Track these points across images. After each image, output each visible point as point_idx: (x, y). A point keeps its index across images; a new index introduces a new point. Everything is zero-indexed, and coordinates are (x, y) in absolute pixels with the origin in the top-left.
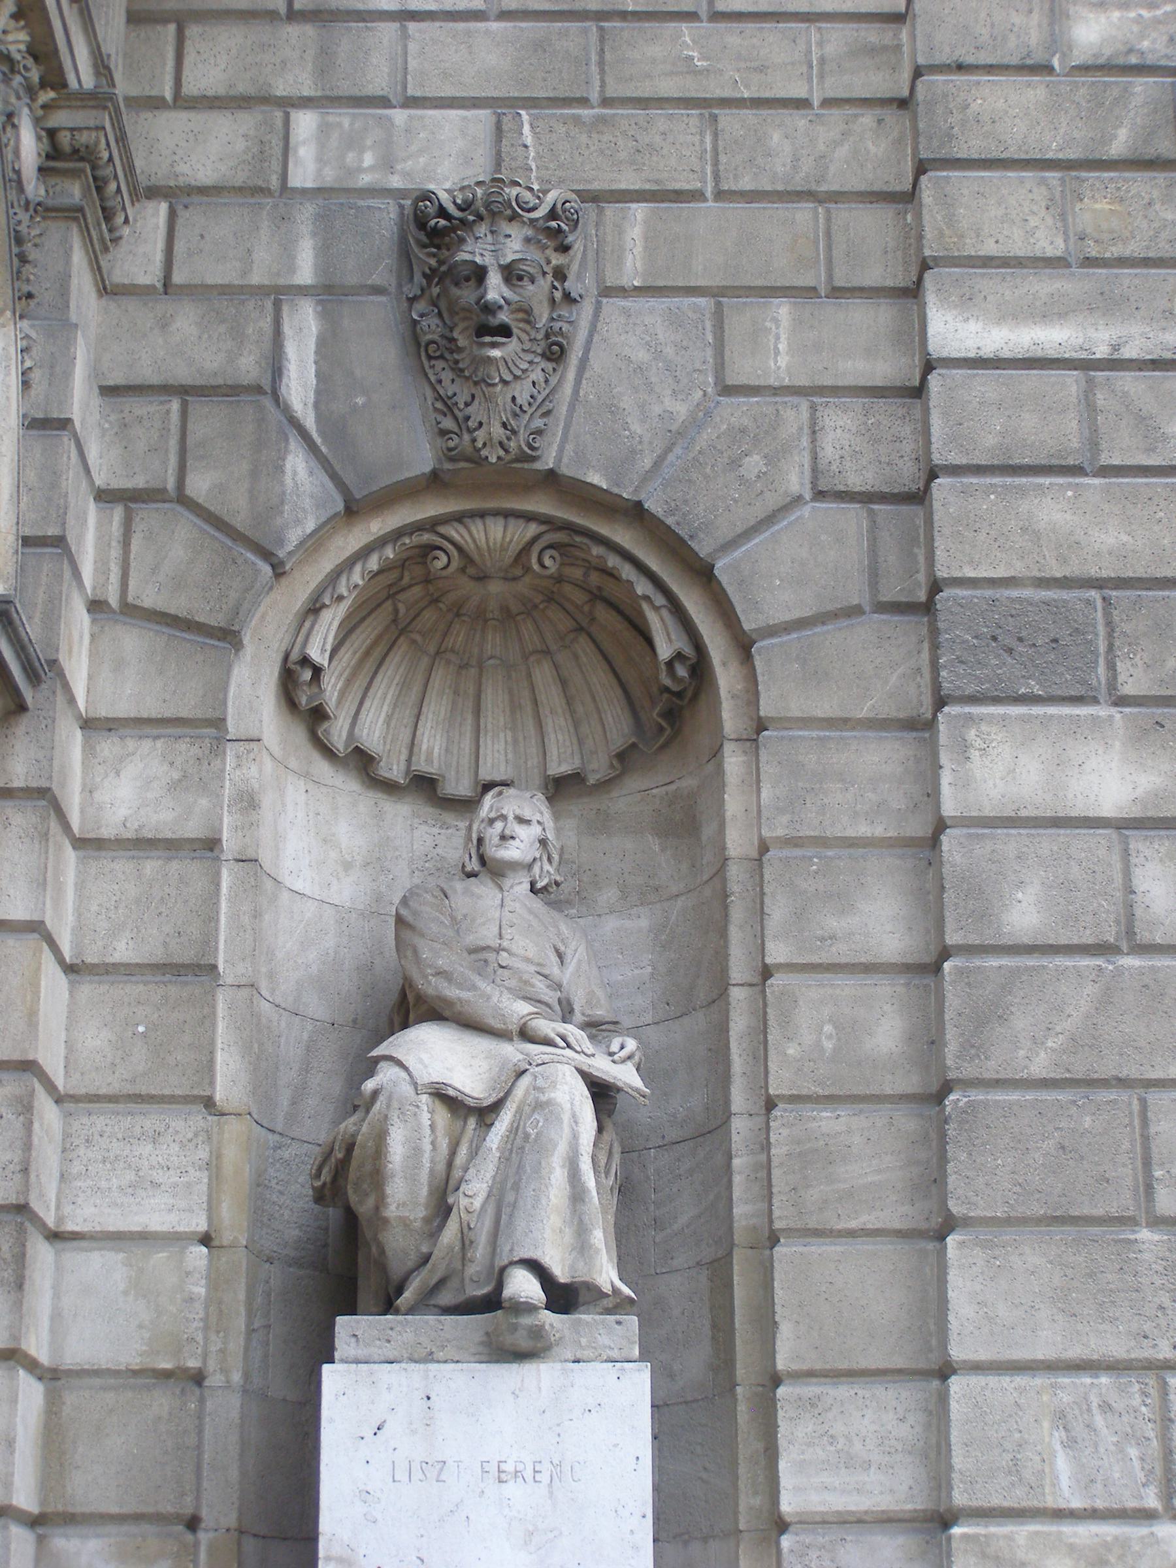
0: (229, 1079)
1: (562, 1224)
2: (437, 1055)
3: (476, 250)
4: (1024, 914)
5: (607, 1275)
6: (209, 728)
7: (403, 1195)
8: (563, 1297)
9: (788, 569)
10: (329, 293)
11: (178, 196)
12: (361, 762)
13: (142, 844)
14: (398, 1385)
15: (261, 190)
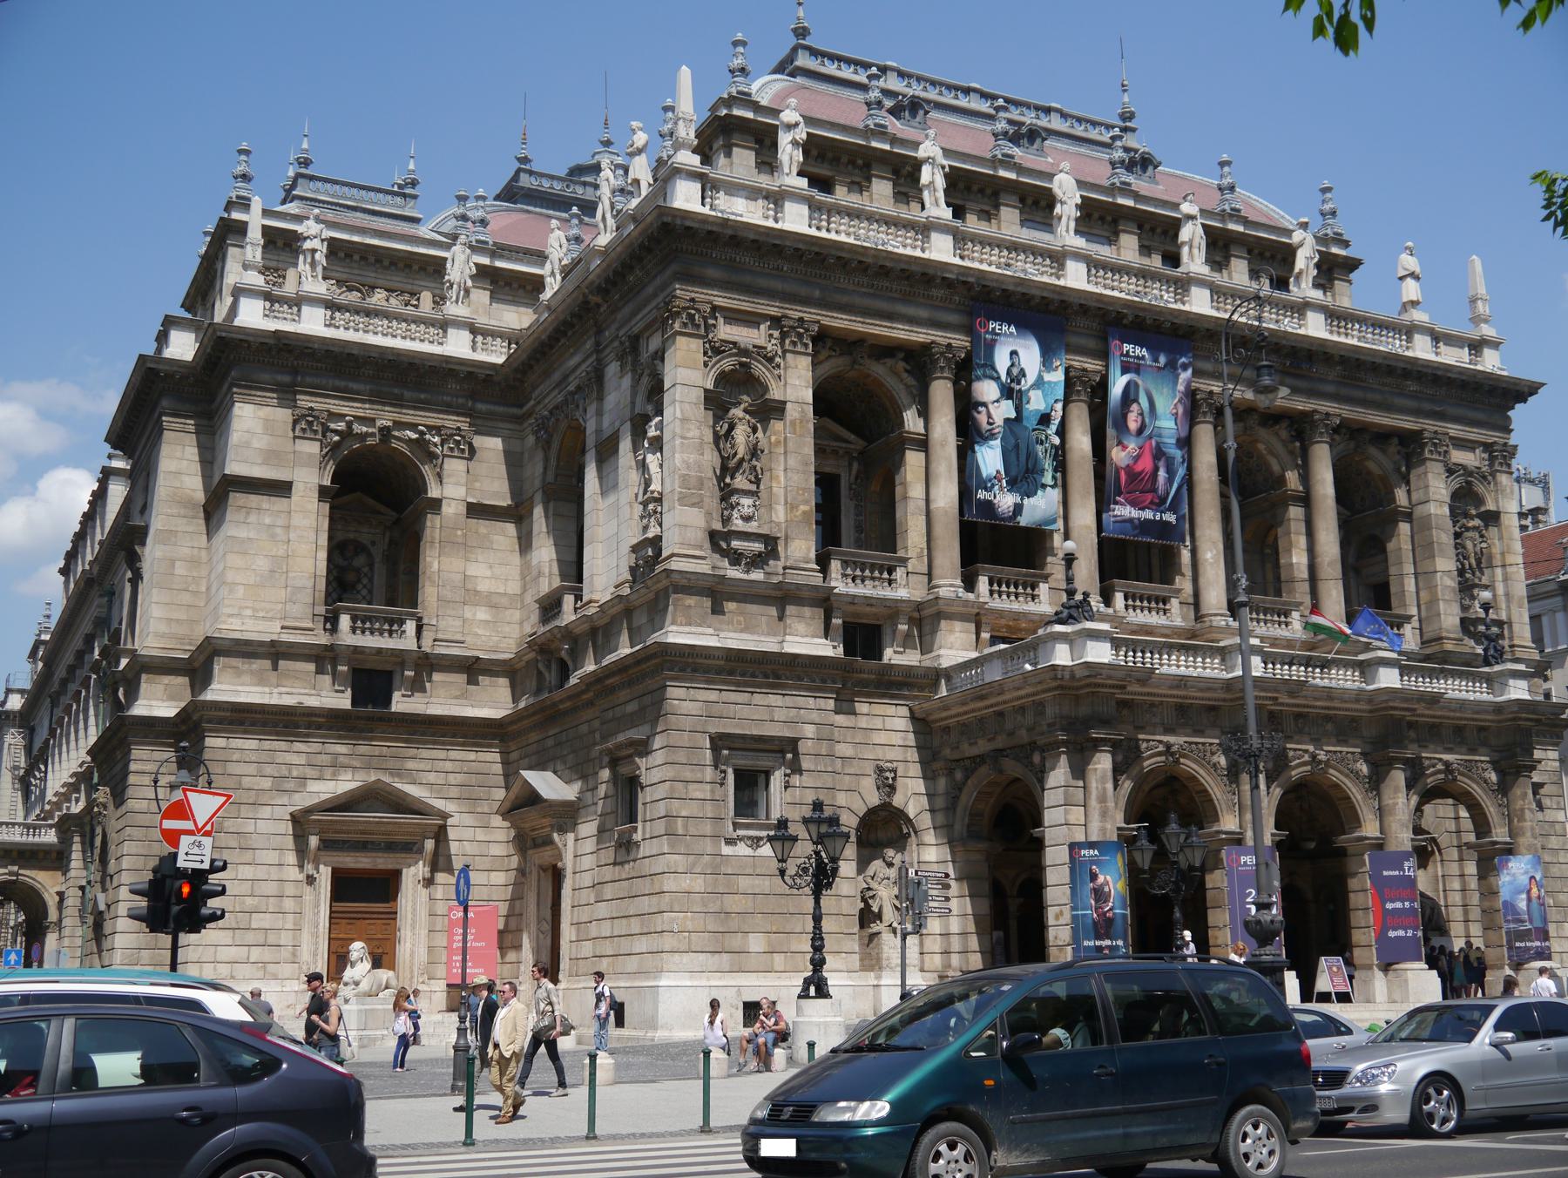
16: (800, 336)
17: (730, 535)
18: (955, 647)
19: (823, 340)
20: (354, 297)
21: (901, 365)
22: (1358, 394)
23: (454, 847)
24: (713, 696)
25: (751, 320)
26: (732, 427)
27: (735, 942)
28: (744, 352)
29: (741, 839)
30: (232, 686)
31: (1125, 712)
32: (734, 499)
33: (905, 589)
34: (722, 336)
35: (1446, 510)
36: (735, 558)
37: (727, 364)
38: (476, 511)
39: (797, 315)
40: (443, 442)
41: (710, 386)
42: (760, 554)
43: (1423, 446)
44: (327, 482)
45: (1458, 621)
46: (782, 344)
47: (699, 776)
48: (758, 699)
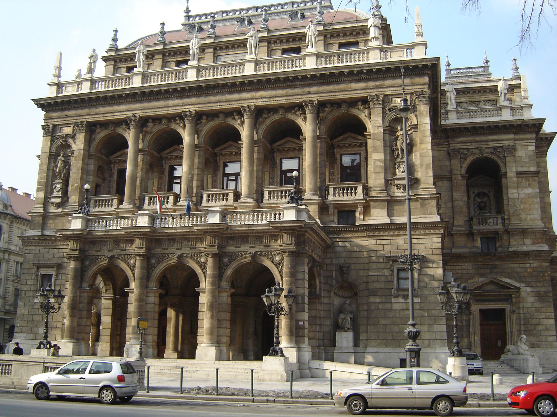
0: (332, 316)
1: (348, 324)
2: (342, 316)
3: (343, 269)
4: (373, 308)
5: (350, 327)
6: (330, 297)
7: (340, 323)
8: (348, 329)
9: (362, 287)
10: (336, 271)
11: (327, 264)
12: (339, 296)
13: (326, 304)
14: (340, 333)
15: (332, 264)
16: (82, 126)
19: (91, 128)
21: (124, 127)
22: (331, 87)
24: (37, 251)
25: (67, 125)
27: (34, 330)
28: (63, 137)
31: (91, 246)
34: (60, 134)
35: (381, 130)
37: (60, 142)
39: (79, 121)
41: (53, 150)
42: (59, 203)
45: (383, 181)
47: (31, 277)
48: (51, 251)
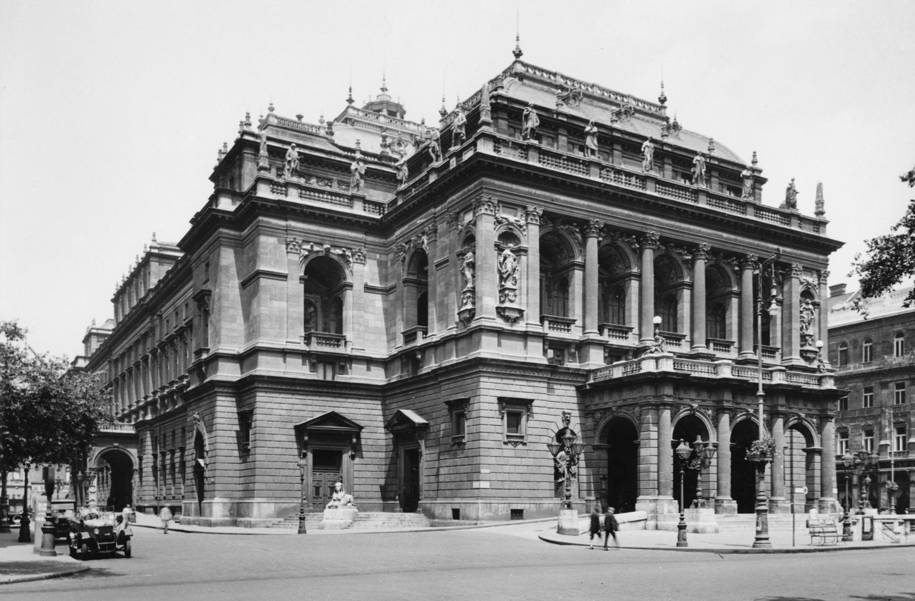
17: (504, 309)
18: (596, 359)
20: (302, 181)
23: (363, 442)
26: (505, 258)
28: (512, 224)
29: (510, 442)
30: (267, 367)
32: (507, 292)
33: (575, 334)
36: (507, 319)
37: (503, 230)
38: (368, 289)
40: (353, 255)
43: (792, 270)
44: (302, 274)
46: (526, 220)
